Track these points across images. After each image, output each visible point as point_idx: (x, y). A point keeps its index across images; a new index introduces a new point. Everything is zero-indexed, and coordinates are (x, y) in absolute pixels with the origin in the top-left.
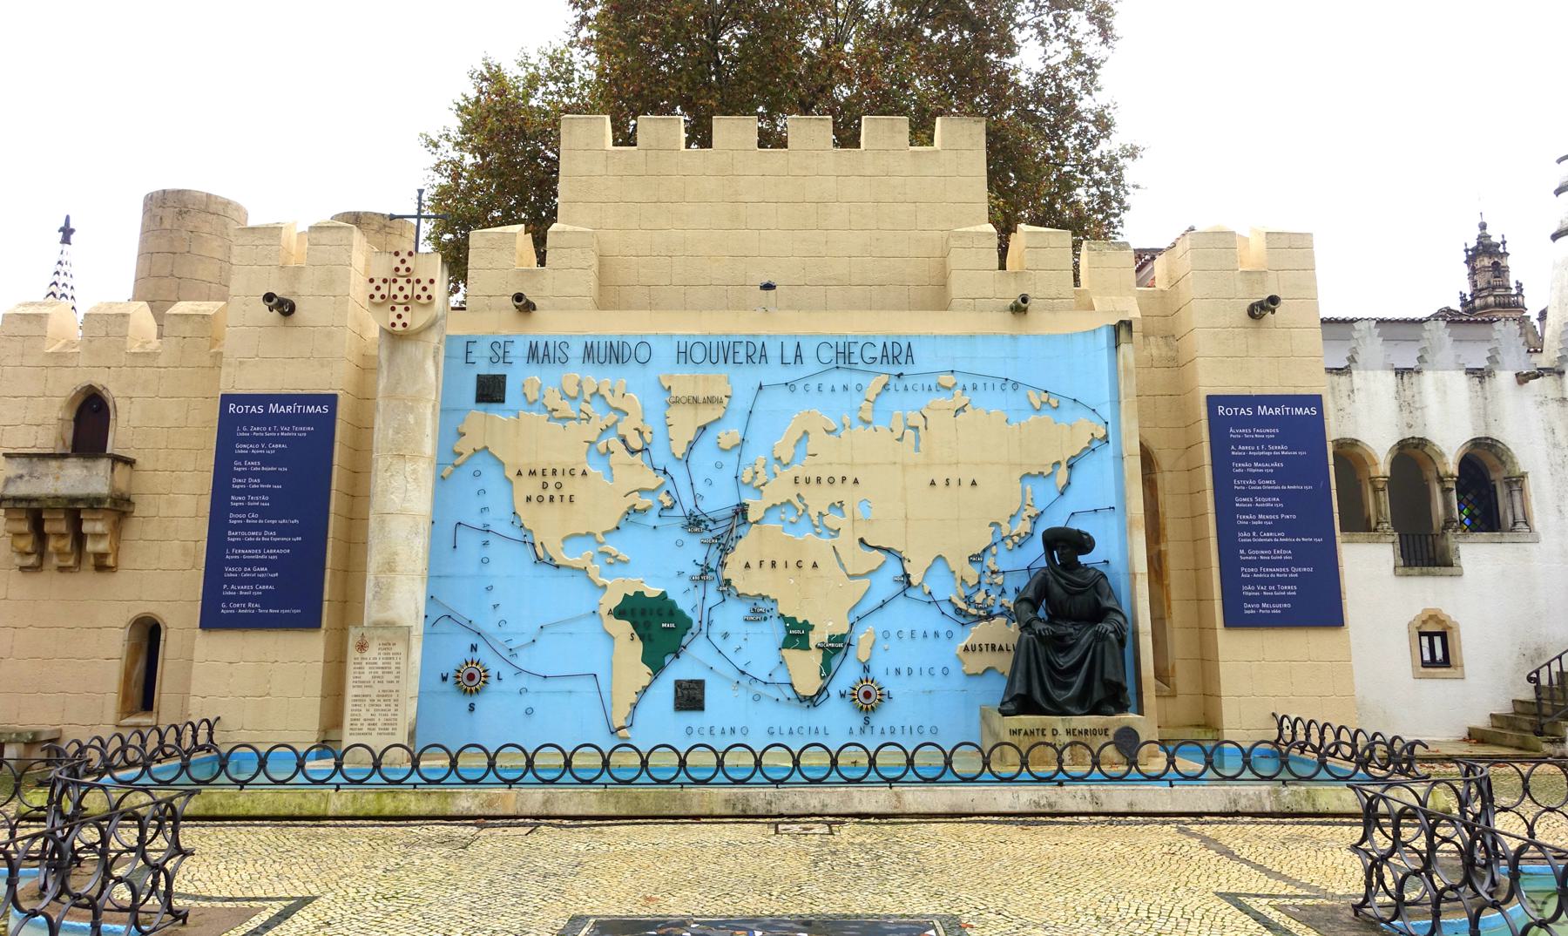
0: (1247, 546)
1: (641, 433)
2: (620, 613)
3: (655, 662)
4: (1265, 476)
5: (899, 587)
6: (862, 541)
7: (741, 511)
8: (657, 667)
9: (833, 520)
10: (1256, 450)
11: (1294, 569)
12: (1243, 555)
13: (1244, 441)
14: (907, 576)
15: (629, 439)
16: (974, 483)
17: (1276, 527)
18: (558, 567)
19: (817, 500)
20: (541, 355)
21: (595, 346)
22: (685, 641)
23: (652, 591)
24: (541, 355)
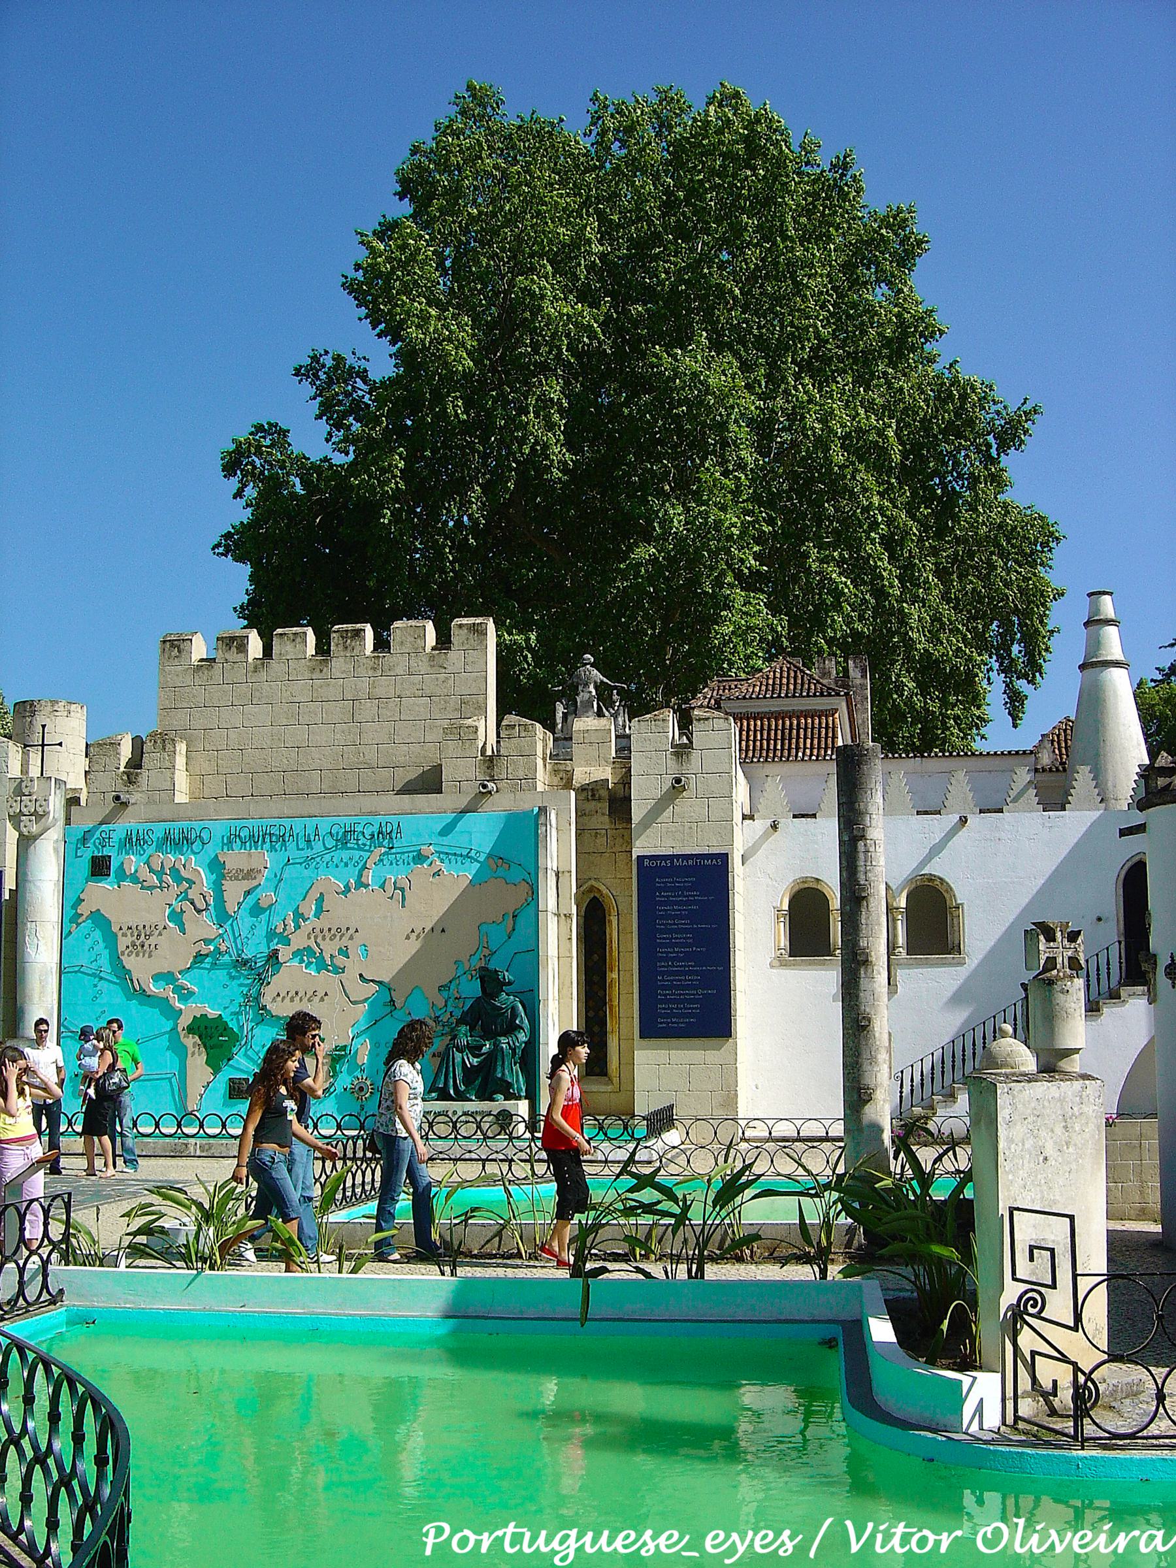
0: (663, 973)
1: (204, 897)
2: (191, 1030)
3: (215, 1065)
4: (681, 917)
5: (388, 1009)
6: (361, 975)
7: (274, 954)
8: (216, 1070)
9: (340, 960)
10: (675, 896)
11: (699, 992)
12: (660, 981)
13: (666, 889)
14: (392, 1000)
15: (196, 902)
16: (443, 931)
17: (688, 956)
18: (149, 996)
19: (330, 948)
20: (134, 840)
21: (172, 832)
22: (235, 1050)
23: (213, 1013)
24: (134, 840)
